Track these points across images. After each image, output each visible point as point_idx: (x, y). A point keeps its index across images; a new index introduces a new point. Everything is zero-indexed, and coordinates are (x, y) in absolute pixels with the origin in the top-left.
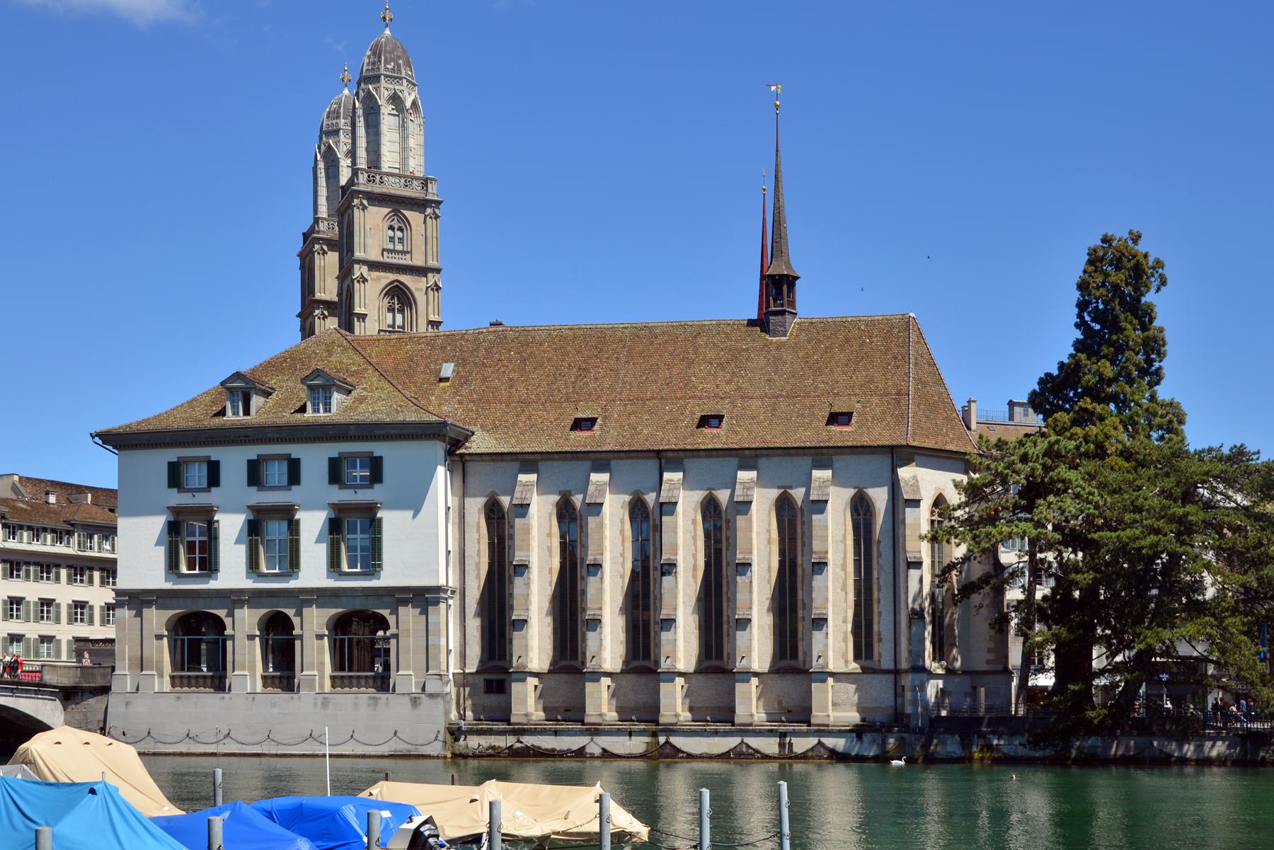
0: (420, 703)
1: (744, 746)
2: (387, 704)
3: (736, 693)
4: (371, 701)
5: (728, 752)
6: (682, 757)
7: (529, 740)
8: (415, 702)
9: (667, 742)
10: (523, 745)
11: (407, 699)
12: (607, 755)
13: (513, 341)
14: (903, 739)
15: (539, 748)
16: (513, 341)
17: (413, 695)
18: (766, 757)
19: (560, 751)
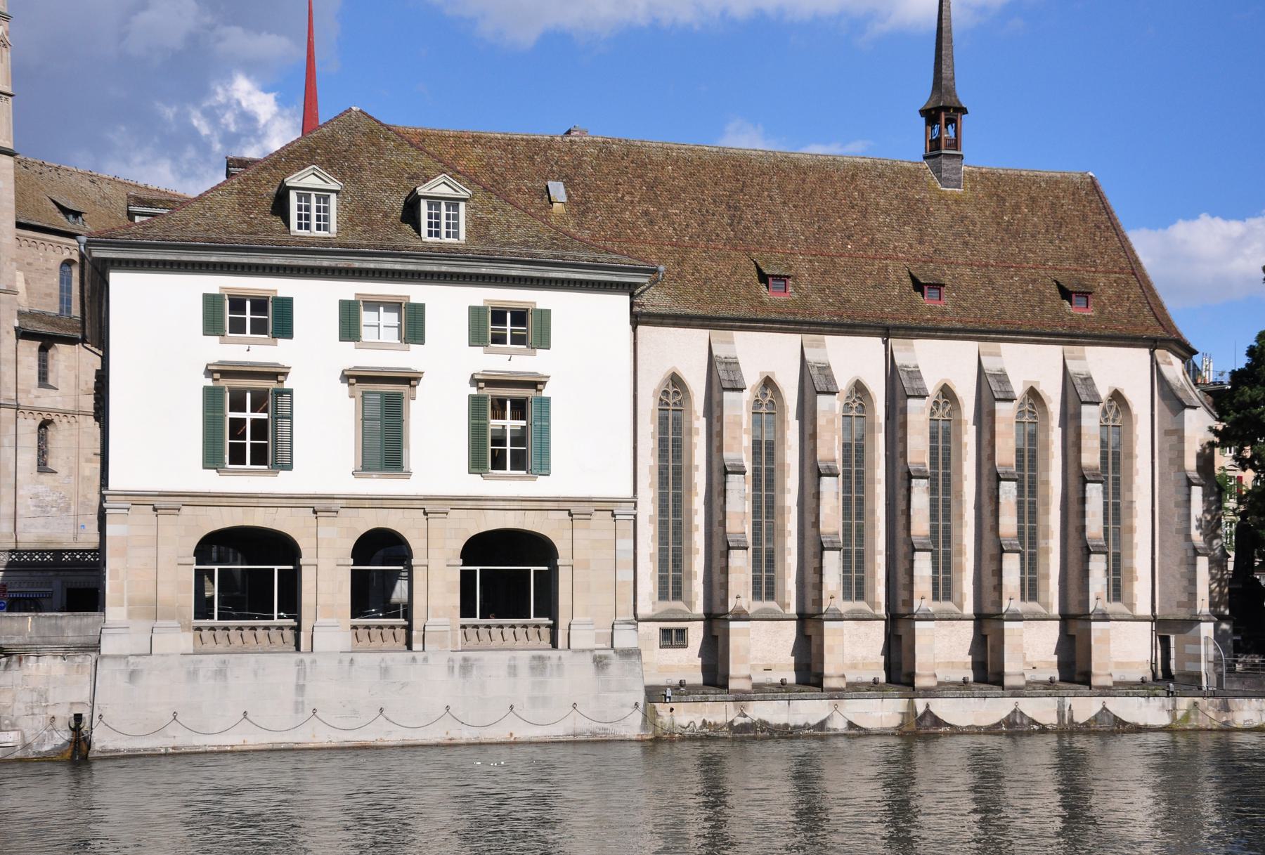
0: (607, 665)
1: (1018, 716)
2: (560, 666)
3: (1005, 646)
4: (535, 663)
5: (999, 724)
6: (945, 734)
7: (762, 711)
8: (600, 663)
9: (928, 712)
10: (747, 720)
11: (588, 658)
12: (856, 732)
13: (623, 159)
14: (1195, 704)
15: (766, 723)
16: (623, 159)
17: (597, 653)
18: (1044, 730)
19: (795, 727)
